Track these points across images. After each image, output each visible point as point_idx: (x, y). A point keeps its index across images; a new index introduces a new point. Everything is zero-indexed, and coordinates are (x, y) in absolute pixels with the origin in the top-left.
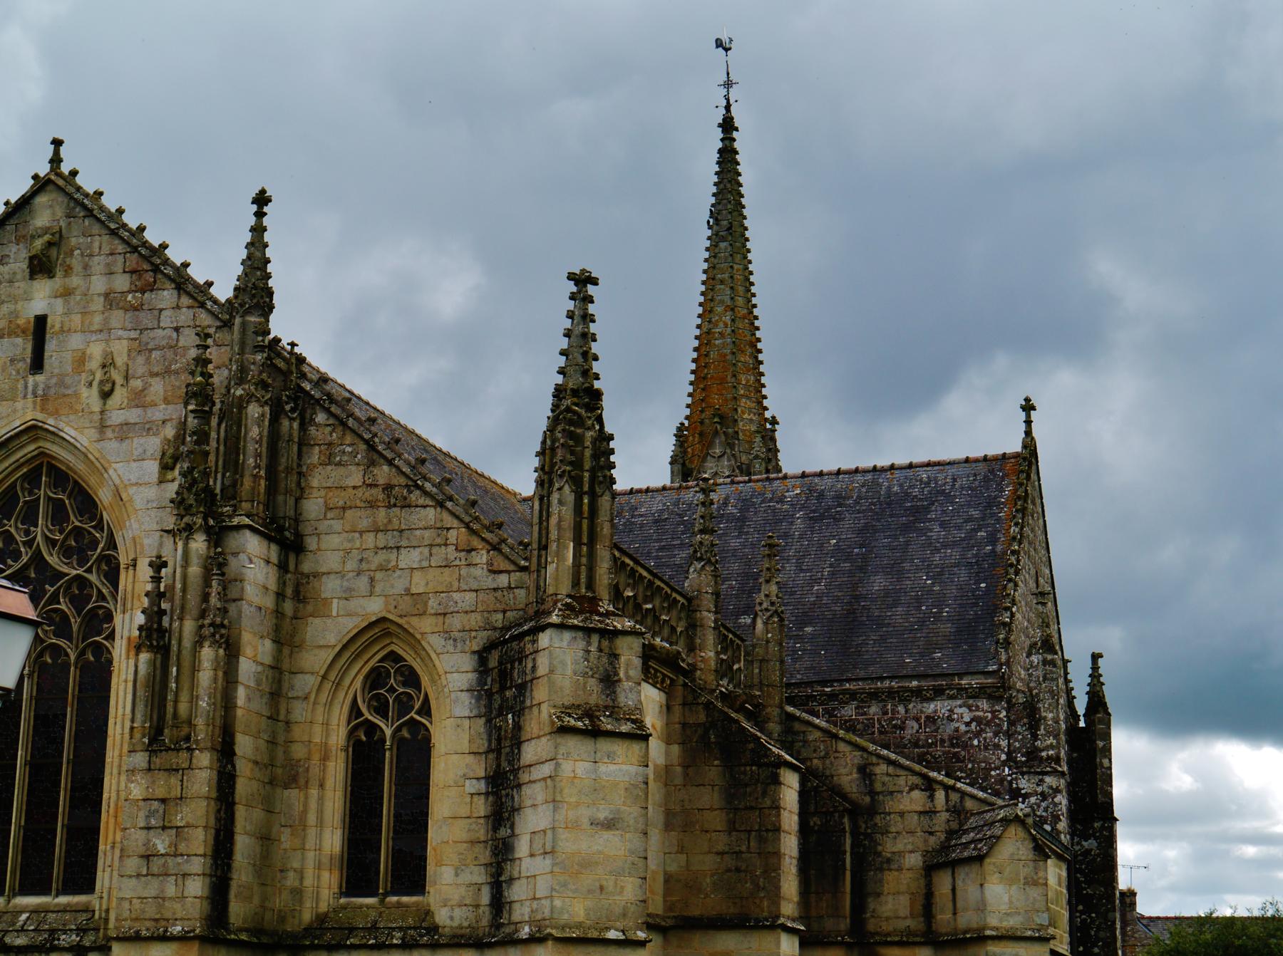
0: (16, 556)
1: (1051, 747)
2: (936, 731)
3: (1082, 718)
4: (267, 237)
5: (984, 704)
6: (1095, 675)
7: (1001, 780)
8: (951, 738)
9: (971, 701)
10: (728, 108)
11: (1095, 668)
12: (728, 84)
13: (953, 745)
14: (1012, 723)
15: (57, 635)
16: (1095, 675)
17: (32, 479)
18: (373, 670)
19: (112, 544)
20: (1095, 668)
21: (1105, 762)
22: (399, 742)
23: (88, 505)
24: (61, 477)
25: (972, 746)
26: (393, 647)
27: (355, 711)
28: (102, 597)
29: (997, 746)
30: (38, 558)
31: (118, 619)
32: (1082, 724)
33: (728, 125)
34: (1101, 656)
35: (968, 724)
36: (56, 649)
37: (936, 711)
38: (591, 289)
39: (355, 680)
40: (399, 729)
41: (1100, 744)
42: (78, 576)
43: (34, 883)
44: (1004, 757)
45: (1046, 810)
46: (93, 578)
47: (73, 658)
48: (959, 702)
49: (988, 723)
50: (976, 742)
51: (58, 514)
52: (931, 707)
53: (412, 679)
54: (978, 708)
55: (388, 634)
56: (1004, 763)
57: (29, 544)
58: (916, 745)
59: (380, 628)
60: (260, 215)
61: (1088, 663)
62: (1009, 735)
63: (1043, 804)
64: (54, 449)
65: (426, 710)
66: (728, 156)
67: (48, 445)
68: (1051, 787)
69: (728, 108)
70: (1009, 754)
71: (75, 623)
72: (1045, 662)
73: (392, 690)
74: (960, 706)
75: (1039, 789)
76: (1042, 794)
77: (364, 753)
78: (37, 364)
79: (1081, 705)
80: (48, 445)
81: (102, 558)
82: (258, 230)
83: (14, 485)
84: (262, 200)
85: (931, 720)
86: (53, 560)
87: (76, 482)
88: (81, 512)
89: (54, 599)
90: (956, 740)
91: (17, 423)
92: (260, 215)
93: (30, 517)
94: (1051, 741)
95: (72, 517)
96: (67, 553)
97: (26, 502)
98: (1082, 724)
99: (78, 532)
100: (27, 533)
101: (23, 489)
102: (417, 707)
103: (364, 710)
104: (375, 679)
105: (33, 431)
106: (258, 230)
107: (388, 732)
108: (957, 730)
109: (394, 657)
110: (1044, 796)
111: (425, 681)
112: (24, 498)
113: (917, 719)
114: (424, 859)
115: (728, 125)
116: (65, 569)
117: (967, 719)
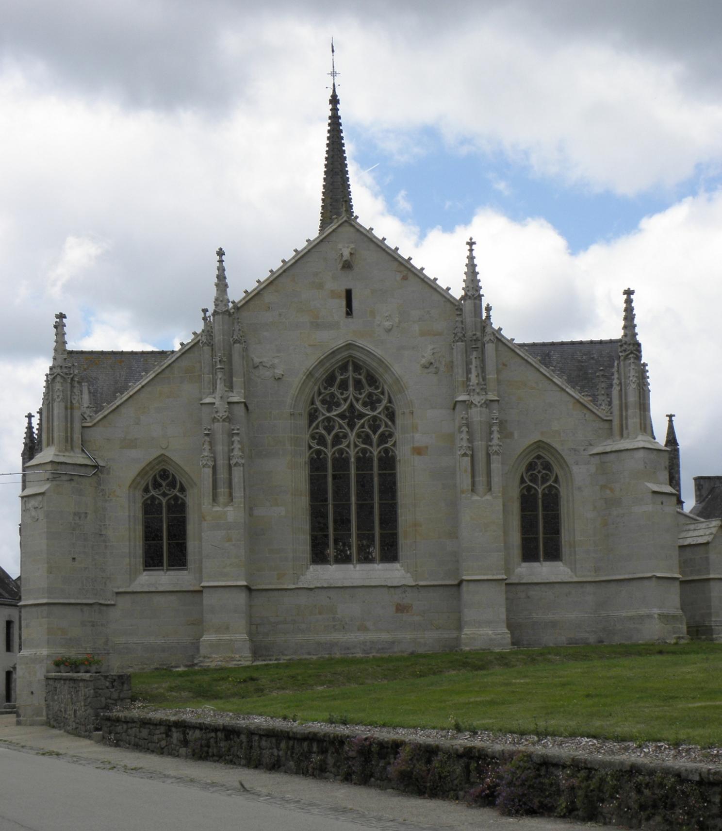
4: (476, 262)
10: (334, 91)
12: (334, 74)
15: (364, 443)
17: (344, 368)
19: (390, 401)
22: (544, 495)
23: (372, 380)
24: (357, 368)
26: (540, 453)
27: (522, 481)
28: (387, 426)
30: (351, 406)
31: (398, 435)
33: (334, 100)
38: (632, 297)
43: (366, 559)
46: (383, 417)
51: (358, 385)
53: (547, 466)
55: (539, 447)
59: (540, 445)
60: (471, 250)
64: (358, 354)
65: (556, 480)
66: (335, 122)
67: (354, 352)
69: (334, 91)
71: (375, 438)
78: (349, 312)
80: (354, 352)
81: (387, 408)
82: (471, 258)
83: (334, 371)
84: (471, 243)
86: (359, 406)
87: (367, 370)
88: (370, 386)
91: (341, 343)
92: (471, 250)
93: (344, 386)
96: (365, 404)
100: (342, 394)
103: (527, 480)
104: (531, 466)
105: (349, 346)
106: (471, 258)
107: (540, 491)
109: (539, 457)
111: (556, 469)
112: (339, 378)
115: (334, 100)
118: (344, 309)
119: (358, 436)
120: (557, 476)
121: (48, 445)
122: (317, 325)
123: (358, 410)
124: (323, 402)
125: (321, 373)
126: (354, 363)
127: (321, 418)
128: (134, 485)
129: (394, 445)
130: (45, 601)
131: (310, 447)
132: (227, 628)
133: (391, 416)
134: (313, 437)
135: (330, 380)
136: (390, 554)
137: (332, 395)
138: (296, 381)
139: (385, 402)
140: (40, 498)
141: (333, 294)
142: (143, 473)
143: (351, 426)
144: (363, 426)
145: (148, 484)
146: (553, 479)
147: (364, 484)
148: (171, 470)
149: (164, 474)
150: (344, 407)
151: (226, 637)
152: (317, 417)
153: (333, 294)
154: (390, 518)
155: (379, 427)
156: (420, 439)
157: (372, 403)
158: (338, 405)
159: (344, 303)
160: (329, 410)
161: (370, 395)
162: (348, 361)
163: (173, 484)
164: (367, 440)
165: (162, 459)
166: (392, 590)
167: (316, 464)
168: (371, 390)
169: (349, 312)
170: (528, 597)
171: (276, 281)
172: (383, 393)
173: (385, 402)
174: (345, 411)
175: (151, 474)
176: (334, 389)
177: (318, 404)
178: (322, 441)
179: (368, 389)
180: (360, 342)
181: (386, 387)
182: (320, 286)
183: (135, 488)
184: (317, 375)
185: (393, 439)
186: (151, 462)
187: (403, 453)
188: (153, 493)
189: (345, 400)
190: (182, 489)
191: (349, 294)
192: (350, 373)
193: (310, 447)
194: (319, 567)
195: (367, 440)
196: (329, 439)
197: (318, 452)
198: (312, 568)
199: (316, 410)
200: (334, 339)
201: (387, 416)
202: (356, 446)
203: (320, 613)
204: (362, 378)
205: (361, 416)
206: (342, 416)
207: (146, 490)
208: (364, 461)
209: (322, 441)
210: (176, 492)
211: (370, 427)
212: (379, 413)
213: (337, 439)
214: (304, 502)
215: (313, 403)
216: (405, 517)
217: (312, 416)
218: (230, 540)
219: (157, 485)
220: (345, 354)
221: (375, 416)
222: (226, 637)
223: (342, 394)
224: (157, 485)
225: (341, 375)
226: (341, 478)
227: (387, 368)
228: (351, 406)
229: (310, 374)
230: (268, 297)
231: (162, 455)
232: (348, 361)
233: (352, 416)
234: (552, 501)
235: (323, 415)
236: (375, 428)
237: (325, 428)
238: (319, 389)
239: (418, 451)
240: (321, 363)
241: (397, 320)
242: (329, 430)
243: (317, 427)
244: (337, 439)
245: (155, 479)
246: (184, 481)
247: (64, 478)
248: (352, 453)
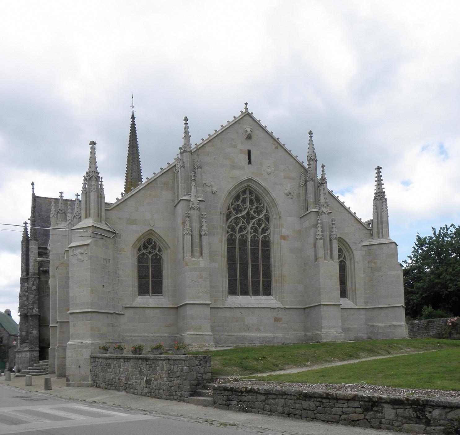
17: (244, 192)
23: (258, 200)
24: (251, 193)
31: (271, 229)
43: (256, 293)
51: (251, 202)
67: (251, 184)
78: (250, 162)
80: (251, 184)
81: (265, 215)
83: (239, 193)
86: (252, 212)
87: (256, 194)
91: (245, 178)
93: (244, 201)
96: (255, 212)
105: (250, 180)
118: (247, 160)
119: (252, 228)
120: (345, 256)
121: (86, 217)
122: (233, 167)
123: (252, 214)
124: (234, 209)
125: (234, 194)
127: (233, 217)
128: (134, 246)
129: (269, 234)
130: (89, 310)
131: (228, 232)
133: (267, 219)
134: (229, 227)
135: (237, 197)
136: (268, 291)
139: (265, 212)
140: (85, 248)
141: (242, 151)
142: (139, 239)
143: (248, 223)
144: (254, 224)
145: (140, 246)
146: (343, 257)
147: (254, 253)
148: (154, 239)
149: (149, 241)
150: (245, 213)
151: (200, 333)
152: (231, 217)
153: (242, 151)
154: (267, 274)
155: (261, 225)
156: (285, 232)
157: (258, 212)
158: (241, 211)
159: (247, 157)
160: (237, 213)
161: (257, 208)
162: (246, 189)
163: (154, 247)
164: (256, 230)
165: (151, 232)
166: (272, 310)
167: (231, 242)
168: (258, 205)
169: (250, 162)
171: (211, 141)
172: (263, 207)
173: (265, 212)
174: (245, 214)
175: (143, 240)
176: (239, 203)
178: (233, 229)
180: (255, 178)
181: (265, 204)
182: (235, 146)
183: (134, 248)
184: (232, 194)
185: (269, 231)
186: (144, 234)
187: (275, 238)
188: (144, 251)
189: (245, 209)
190: (160, 250)
191: (249, 152)
192: (247, 195)
194: (233, 297)
195: (256, 230)
197: (231, 235)
198: (230, 297)
199: (230, 213)
201: (265, 219)
202: (251, 233)
203: (237, 321)
204: (253, 197)
206: (243, 217)
207: (139, 250)
208: (254, 242)
209: (233, 229)
210: (156, 251)
211: (257, 224)
212: (262, 217)
213: (241, 229)
214: (225, 261)
216: (275, 273)
217: (228, 216)
218: (201, 278)
219: (145, 247)
220: (246, 184)
221: (260, 219)
222: (200, 333)
223: (243, 206)
224: (145, 247)
225: (243, 195)
226: (243, 250)
227: (268, 193)
228: (248, 213)
230: (208, 149)
231: (151, 230)
232: (246, 189)
233: (248, 218)
236: (260, 225)
237: (235, 223)
238: (232, 202)
239: (284, 238)
240: (235, 188)
241: (273, 169)
243: (231, 222)
244: (241, 229)
245: (144, 245)
246: (161, 246)
247: (99, 237)
248: (249, 236)
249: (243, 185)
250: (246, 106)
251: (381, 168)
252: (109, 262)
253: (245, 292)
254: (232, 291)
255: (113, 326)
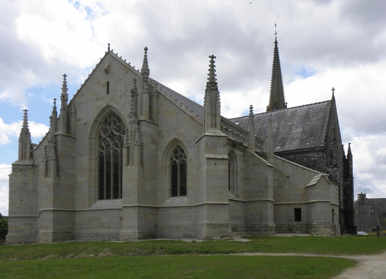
0: (108, 132)
1: (335, 162)
2: (310, 160)
3: (346, 157)
5: (320, 153)
6: (349, 148)
7: (324, 170)
8: (314, 161)
9: (318, 153)
11: (349, 146)
13: (314, 163)
14: (327, 157)
16: (349, 148)
17: (110, 116)
18: (174, 150)
20: (349, 146)
21: (351, 166)
23: (120, 120)
24: (115, 115)
25: (318, 162)
27: (172, 158)
29: (324, 162)
32: (346, 158)
34: (350, 143)
35: (317, 158)
36: (116, 150)
37: (310, 156)
39: (171, 152)
40: (180, 162)
41: (350, 162)
42: (119, 135)
44: (325, 164)
45: (334, 175)
47: (119, 152)
48: (316, 153)
49: (321, 157)
50: (319, 162)
51: (115, 123)
52: (309, 155)
53: (183, 151)
54: (319, 155)
56: (325, 166)
57: (110, 129)
58: (306, 163)
61: (348, 145)
62: (326, 160)
63: (334, 174)
64: (113, 110)
65: (185, 157)
68: (335, 170)
70: (326, 164)
71: (119, 144)
72: (334, 144)
73: (179, 153)
74: (315, 154)
75: (333, 171)
76: (333, 172)
77: (174, 168)
79: (346, 154)
83: (107, 118)
85: (309, 157)
86: (114, 132)
87: (118, 116)
89: (115, 140)
90: (315, 161)
91: (105, 105)
93: (110, 124)
94: (335, 160)
95: (117, 123)
97: (109, 121)
98: (346, 158)
99: (119, 126)
100: (110, 127)
101: (109, 118)
102: (183, 157)
104: (176, 151)
105: (108, 106)
108: (315, 159)
110: (334, 172)
112: (109, 120)
113: (306, 158)
114: (186, 188)
116: (117, 134)
117: (317, 157)
118: (106, 91)
124: (104, 131)
126: (112, 112)
132: (48, 228)
135: (106, 122)
137: (107, 129)
138: (90, 124)
158: (108, 132)
166: (119, 210)
169: (108, 92)
170: (169, 214)
172: (122, 125)
174: (110, 134)
177: (102, 133)
179: (118, 124)
192: (112, 118)
193: (99, 151)
196: (105, 147)
200: (102, 104)
205: (116, 135)
215: (100, 132)
229: (96, 121)
230: (83, 91)
234: (183, 167)
235: (103, 137)
238: (102, 127)
240: (99, 115)
242: (105, 143)
249: (106, 111)
250: (109, 46)
251: (215, 57)
252: (28, 184)
253: (108, 197)
254: (101, 197)
255: (30, 225)
